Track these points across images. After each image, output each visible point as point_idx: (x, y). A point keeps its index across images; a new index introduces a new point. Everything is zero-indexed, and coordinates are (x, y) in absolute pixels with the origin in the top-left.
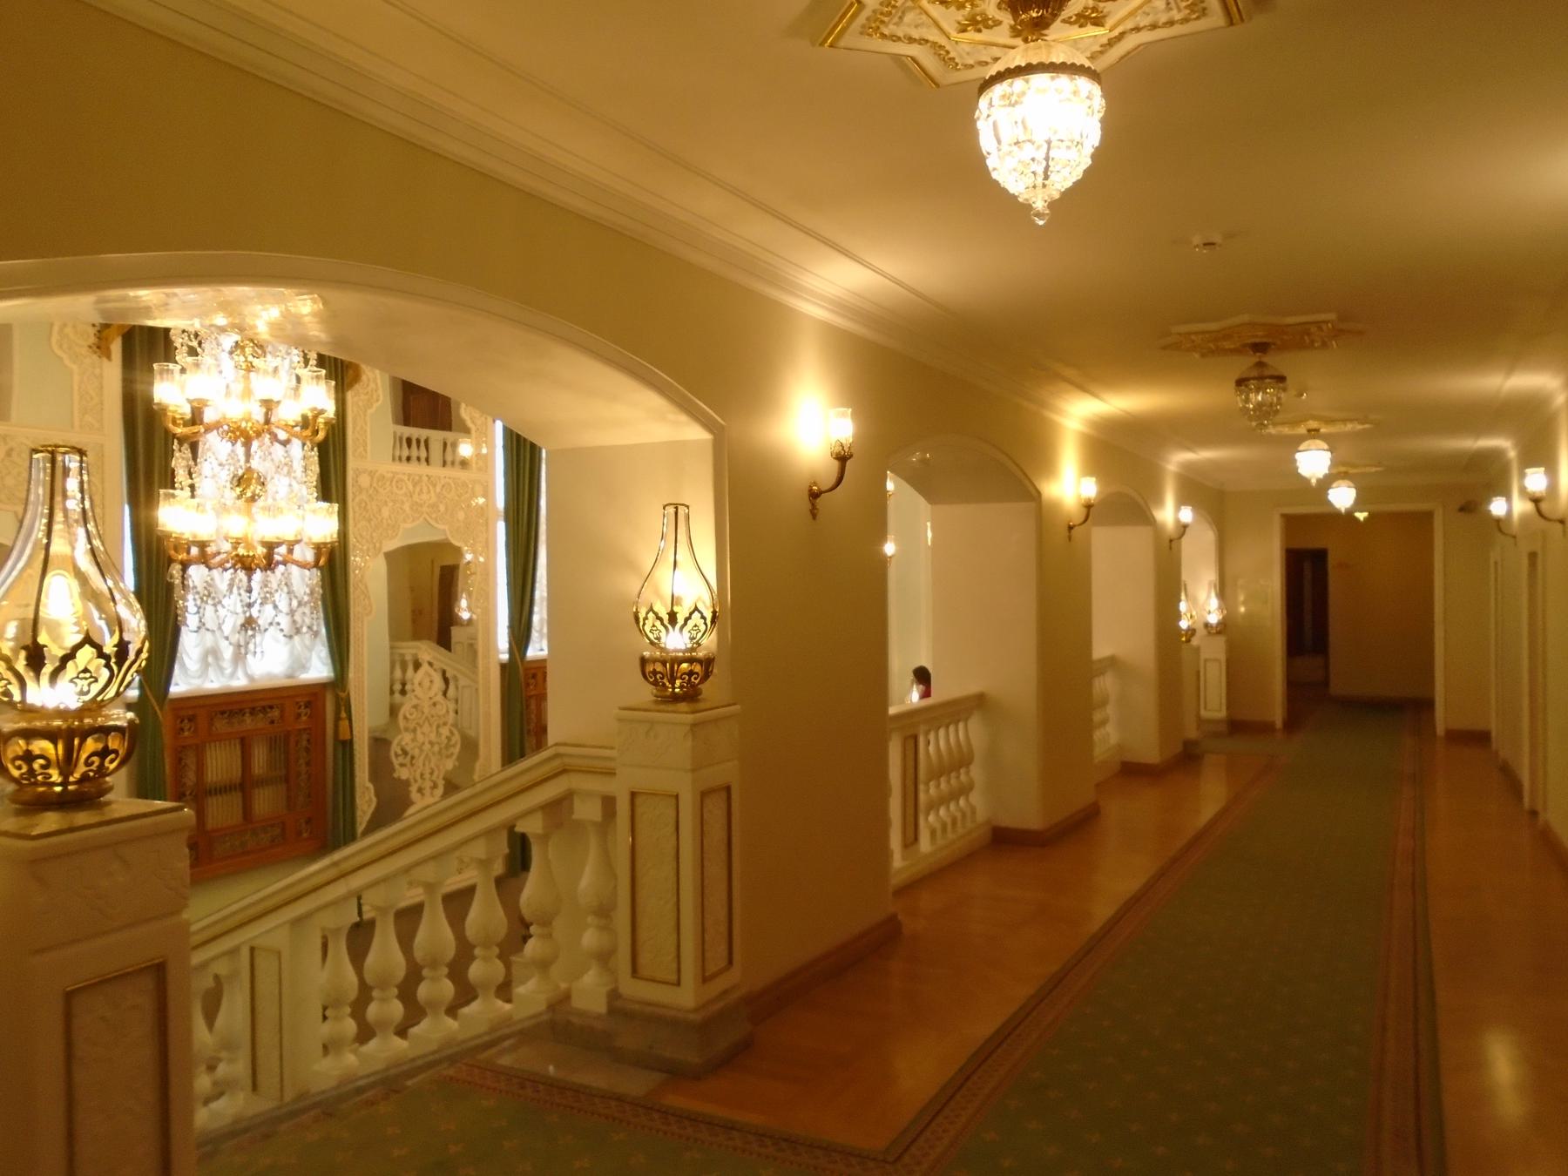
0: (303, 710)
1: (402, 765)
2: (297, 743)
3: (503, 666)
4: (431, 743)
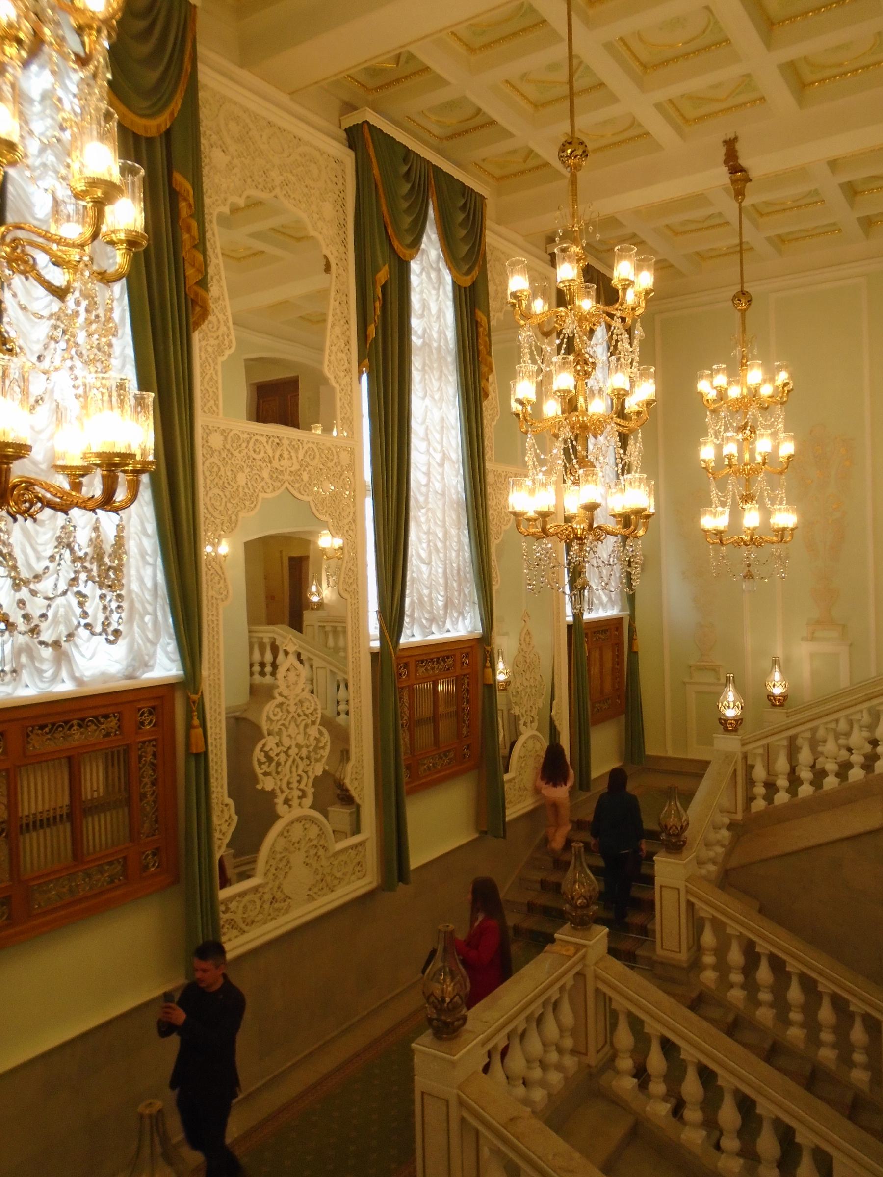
0: (146, 718)
1: (266, 774)
2: (140, 757)
3: (374, 656)
4: (298, 746)
